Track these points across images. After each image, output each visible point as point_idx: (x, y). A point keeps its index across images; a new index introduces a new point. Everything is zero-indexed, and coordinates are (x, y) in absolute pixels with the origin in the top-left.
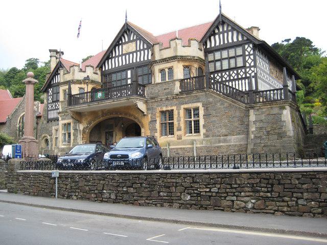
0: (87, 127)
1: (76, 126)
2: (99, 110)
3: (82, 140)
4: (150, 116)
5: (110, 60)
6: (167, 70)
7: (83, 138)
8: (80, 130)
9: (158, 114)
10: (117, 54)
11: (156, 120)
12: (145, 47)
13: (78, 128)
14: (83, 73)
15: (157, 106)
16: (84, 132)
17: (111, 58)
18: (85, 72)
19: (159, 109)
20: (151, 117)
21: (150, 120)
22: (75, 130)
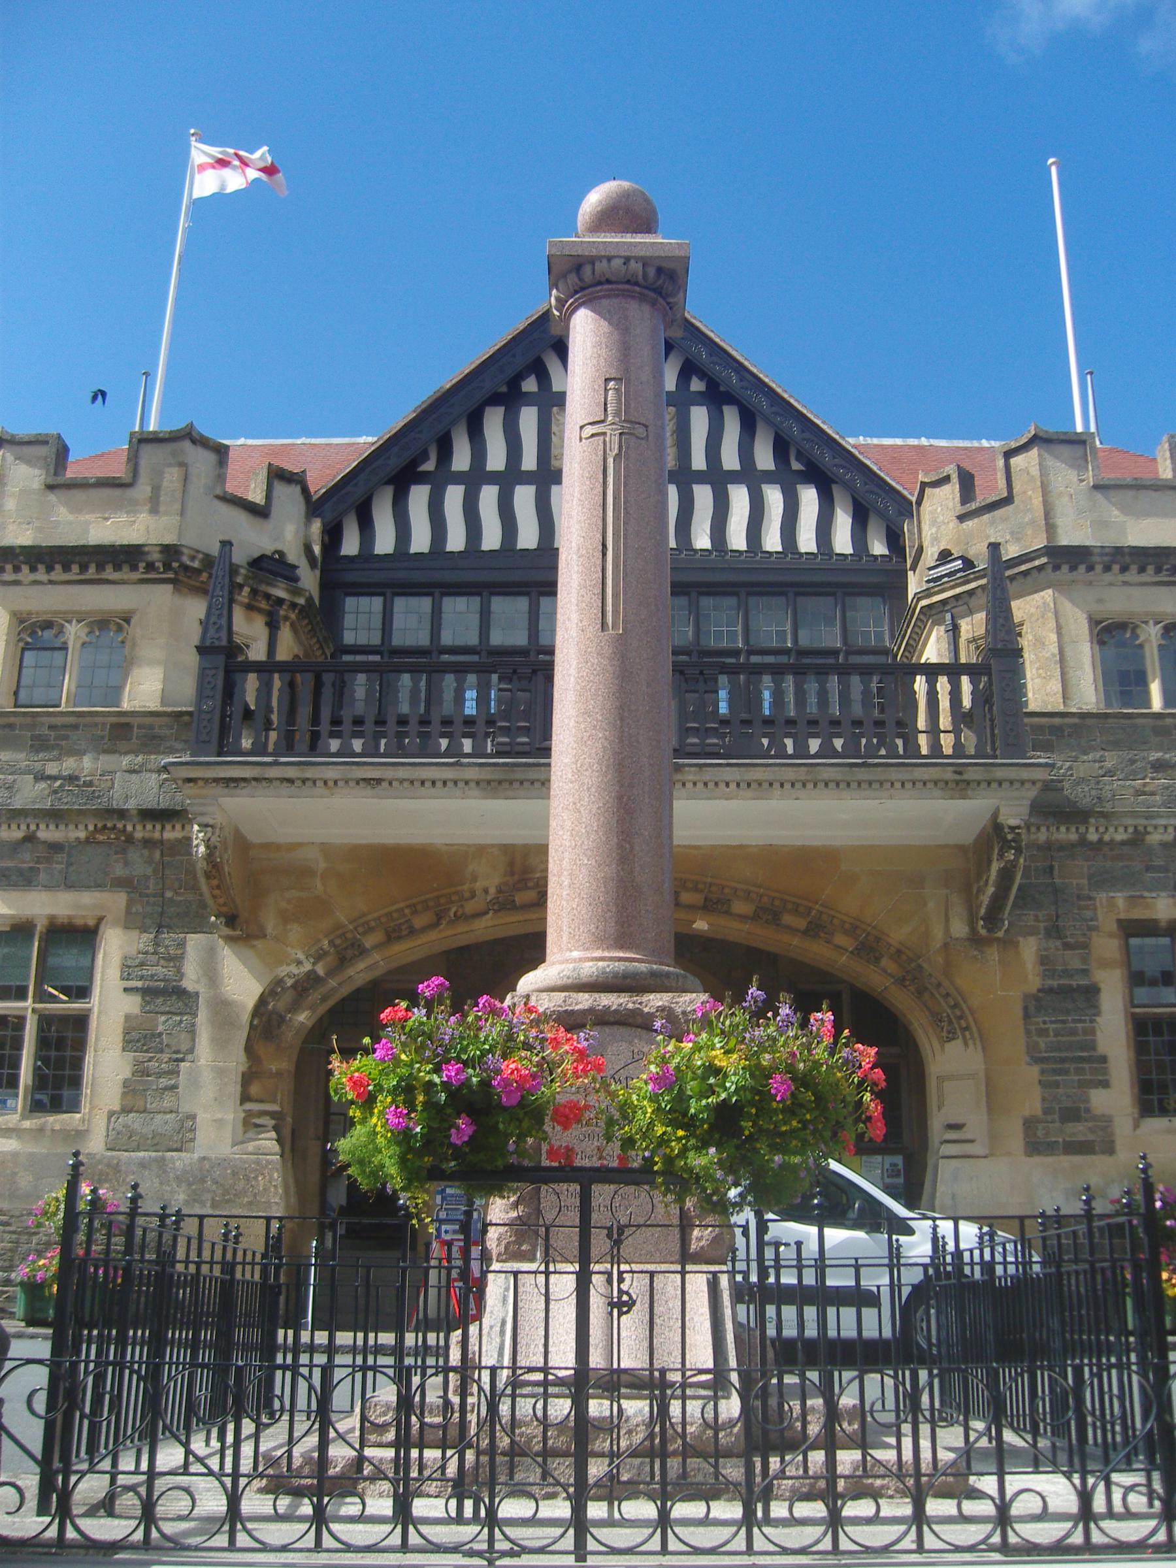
0: (311, 981)
1: (176, 960)
2: (481, 850)
3: (245, 1098)
4: (1029, 949)
5: (419, 496)
6: (1152, 635)
7: (247, 1079)
8: (222, 1008)
9: (1107, 946)
10: (496, 460)
11: (1092, 992)
12: (765, 459)
13: (192, 978)
14: (241, 518)
15: (1102, 880)
16: (266, 1022)
17: (439, 482)
18: (260, 512)
19: (1114, 905)
20: (1043, 960)
21: (1034, 982)
22: (164, 994)
